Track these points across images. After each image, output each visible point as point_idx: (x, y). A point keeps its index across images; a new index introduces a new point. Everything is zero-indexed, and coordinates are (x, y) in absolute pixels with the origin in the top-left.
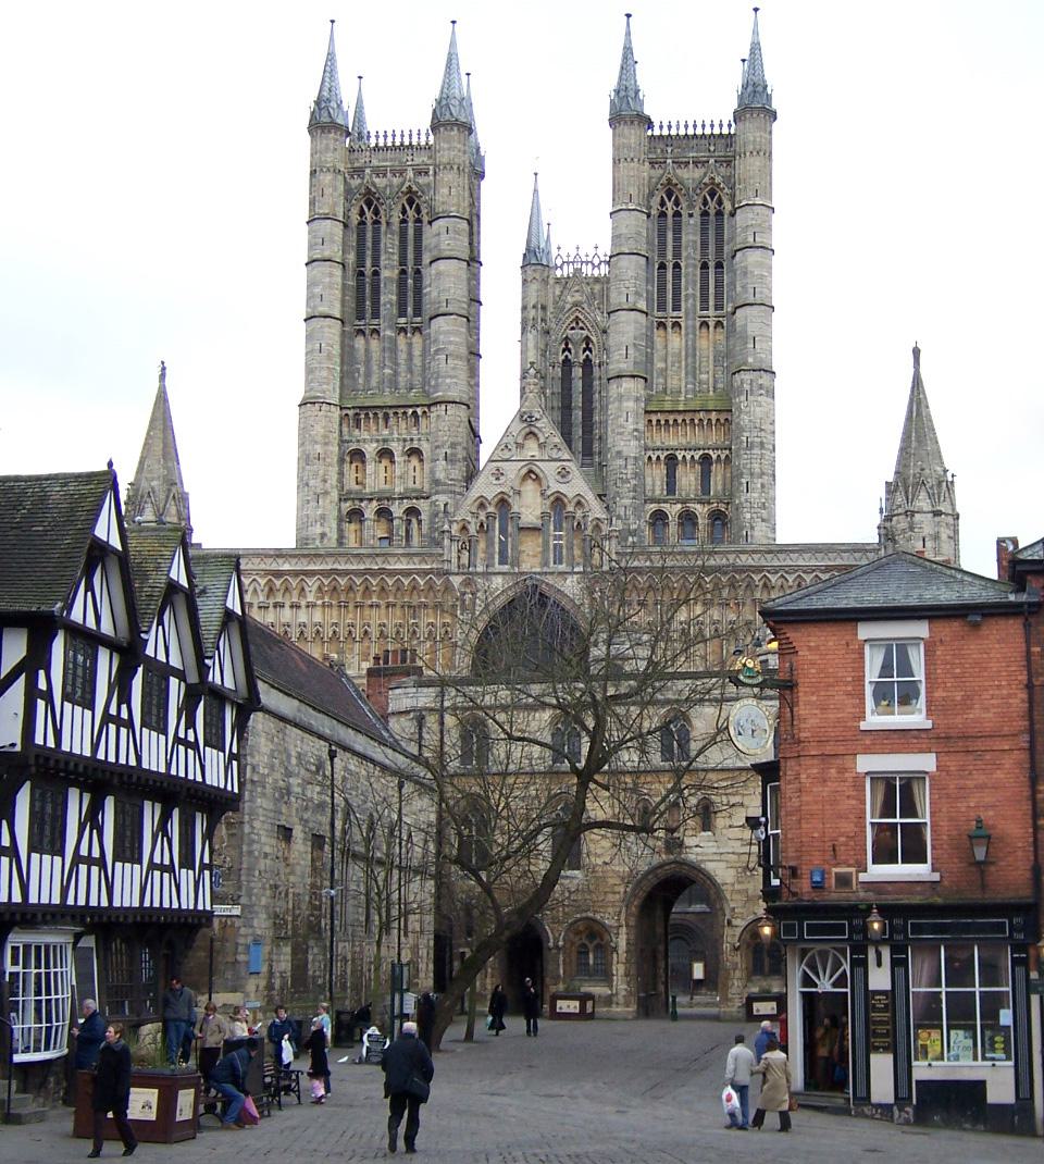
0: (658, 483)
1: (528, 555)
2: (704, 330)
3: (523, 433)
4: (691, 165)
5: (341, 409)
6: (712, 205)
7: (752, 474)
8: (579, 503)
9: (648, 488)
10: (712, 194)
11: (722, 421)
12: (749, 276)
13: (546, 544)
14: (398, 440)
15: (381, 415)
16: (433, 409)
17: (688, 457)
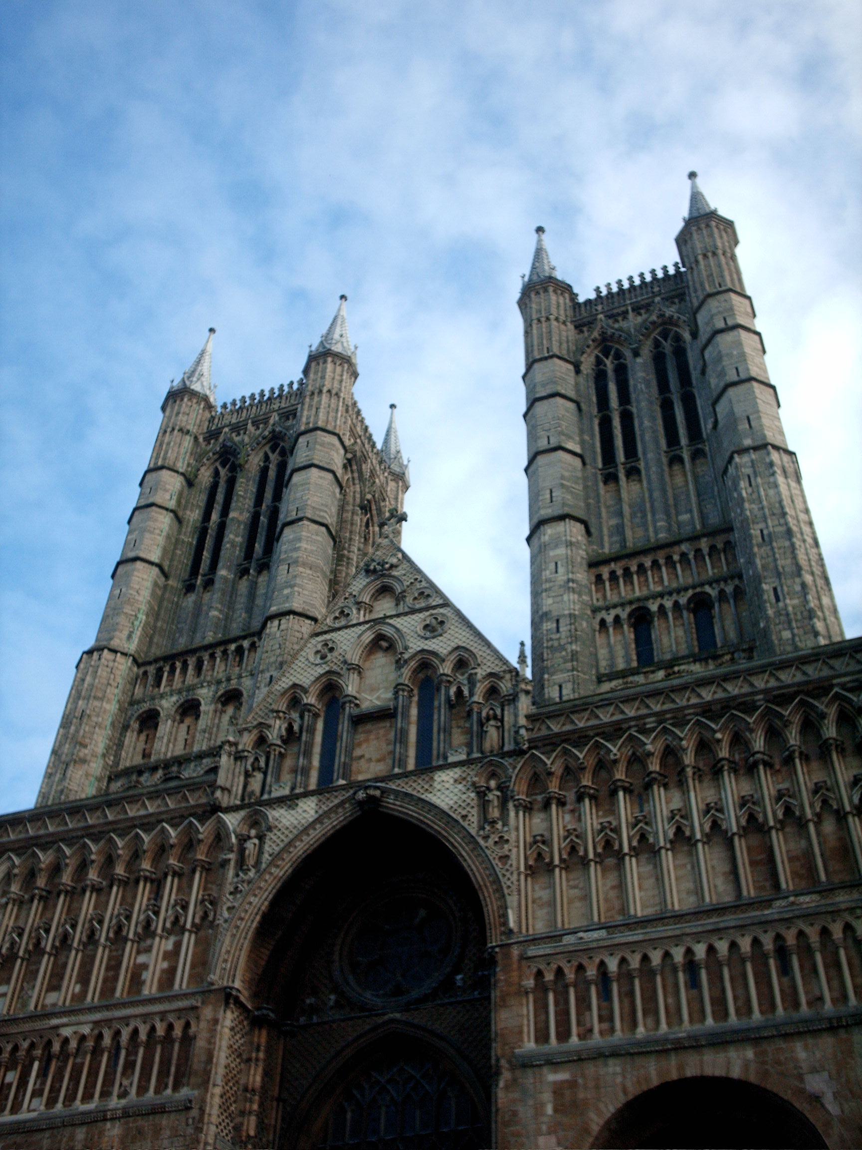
0: (620, 652)
1: (370, 760)
2: (676, 468)
3: (372, 589)
4: (631, 315)
5: (139, 665)
6: (668, 347)
7: (779, 575)
8: (461, 664)
9: (603, 664)
10: (665, 335)
11: (720, 546)
12: (725, 358)
13: (402, 737)
14: (210, 684)
15: (192, 662)
16: (264, 636)
17: (668, 604)
